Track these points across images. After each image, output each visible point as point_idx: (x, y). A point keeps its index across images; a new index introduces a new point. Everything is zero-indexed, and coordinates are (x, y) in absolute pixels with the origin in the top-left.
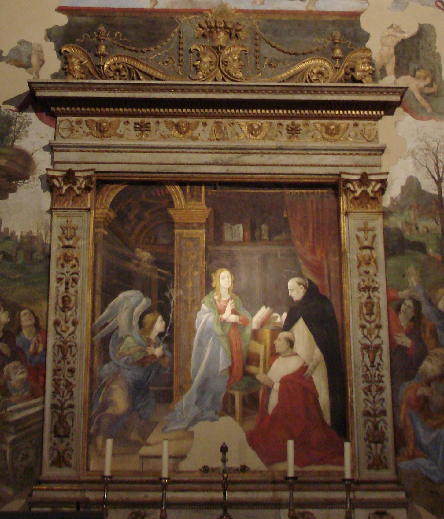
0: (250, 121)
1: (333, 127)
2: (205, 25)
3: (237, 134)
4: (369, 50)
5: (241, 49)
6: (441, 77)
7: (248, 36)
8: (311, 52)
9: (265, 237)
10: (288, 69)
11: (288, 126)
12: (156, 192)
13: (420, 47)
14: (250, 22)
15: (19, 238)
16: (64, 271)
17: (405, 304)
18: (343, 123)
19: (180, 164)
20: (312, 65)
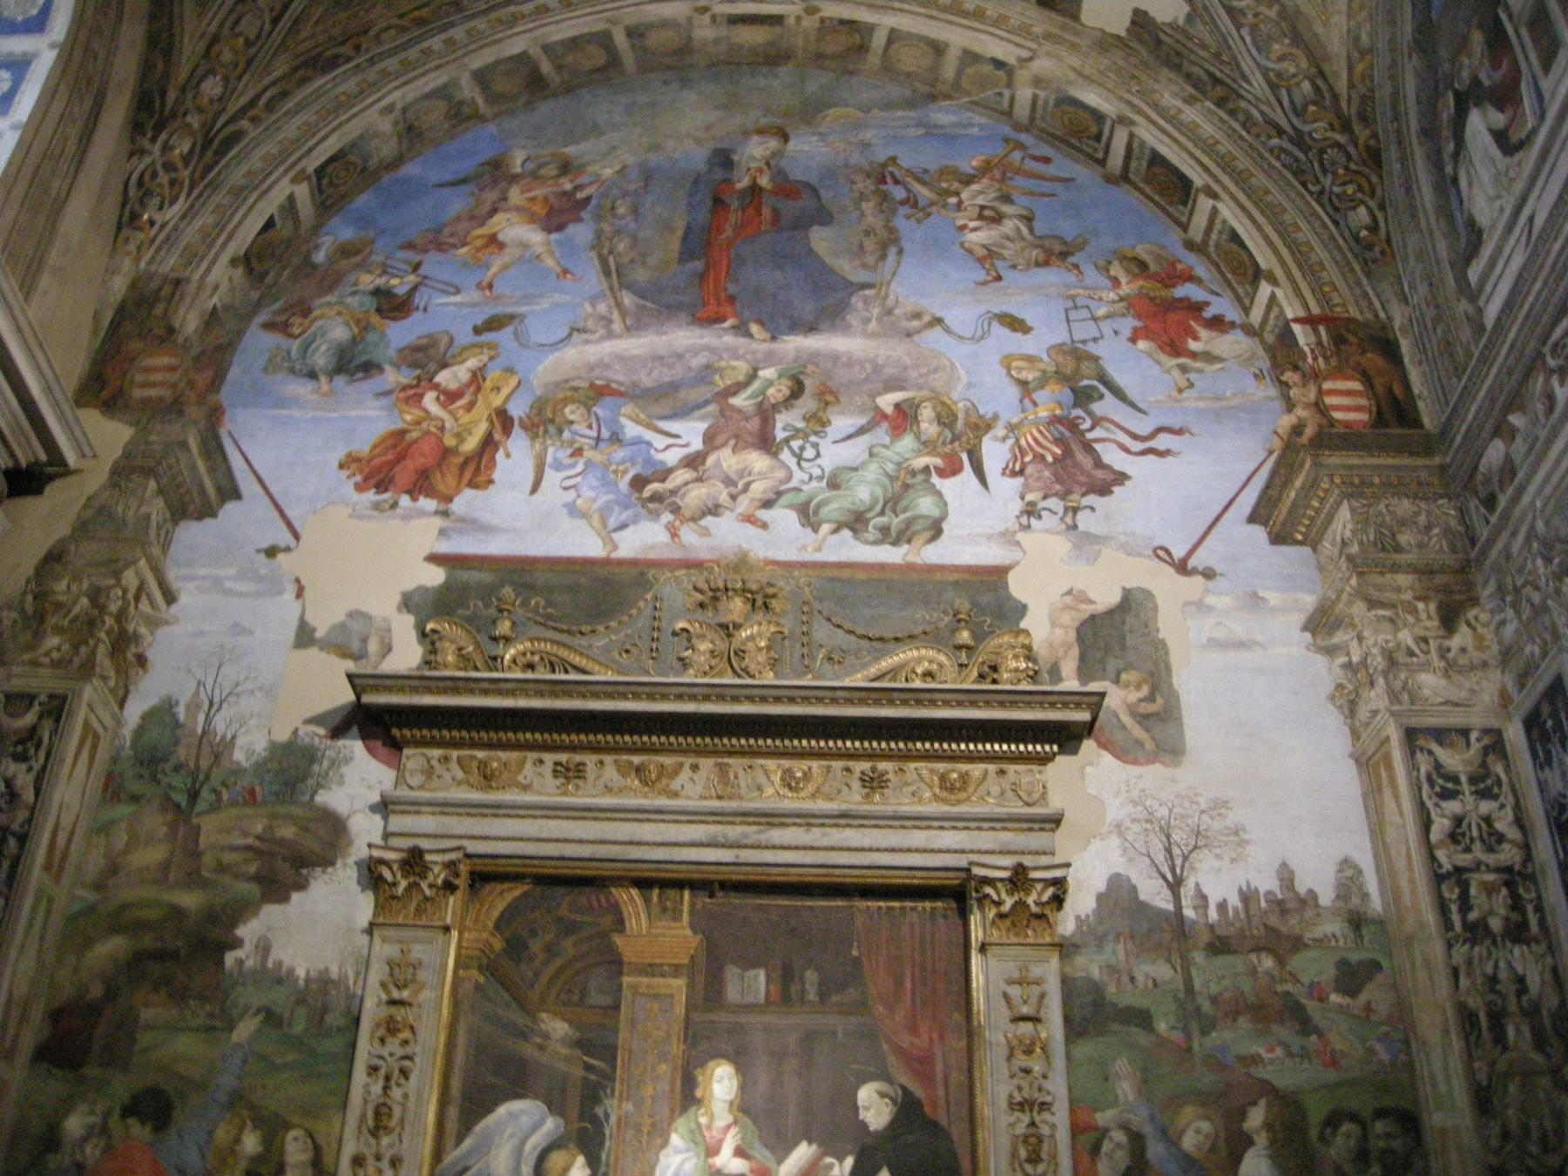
0: (786, 763)
1: (955, 776)
2: (705, 587)
3: (760, 788)
4: (1026, 633)
5: (773, 629)
6: (1170, 685)
7: (789, 607)
8: (911, 637)
9: (812, 996)
10: (865, 666)
11: (863, 773)
12: (589, 900)
13: (1127, 628)
15: (301, 982)
16: (385, 1052)
17: (1111, 1139)
18: (976, 769)
19: (639, 843)
20: (913, 659)
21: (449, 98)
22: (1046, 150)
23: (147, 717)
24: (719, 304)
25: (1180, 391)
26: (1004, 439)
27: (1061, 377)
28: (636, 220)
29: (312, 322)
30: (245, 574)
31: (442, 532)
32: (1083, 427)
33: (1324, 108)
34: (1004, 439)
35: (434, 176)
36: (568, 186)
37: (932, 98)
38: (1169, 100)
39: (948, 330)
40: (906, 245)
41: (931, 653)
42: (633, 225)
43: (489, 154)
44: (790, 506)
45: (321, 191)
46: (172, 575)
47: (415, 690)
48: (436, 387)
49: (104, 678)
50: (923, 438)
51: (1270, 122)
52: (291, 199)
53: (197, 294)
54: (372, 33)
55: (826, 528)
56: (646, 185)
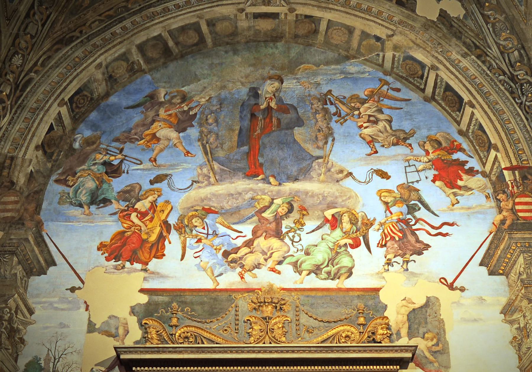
2: (256, 301)
4: (387, 318)
7: (290, 308)
13: (428, 314)
14: (291, 298)
21: (127, 60)
22: (398, 85)
23: (28, 365)
24: (256, 168)
25: (453, 205)
26: (378, 230)
27: (403, 200)
28: (217, 126)
29: (77, 179)
30: (63, 300)
31: (145, 279)
32: (411, 223)
33: (524, 64)
34: (378, 230)
35: (125, 103)
36: (186, 108)
37: (347, 58)
38: (455, 56)
39: (354, 178)
40: (336, 135)
41: (349, 328)
42: (216, 128)
43: (148, 92)
44: (289, 264)
45: (73, 111)
46: (30, 301)
47: (141, 352)
48: (136, 210)
49: (6, 349)
50: (344, 230)
51: (500, 68)
52: (59, 113)
53: (22, 166)
54: (87, 25)
55: (305, 273)
56: (221, 107)
